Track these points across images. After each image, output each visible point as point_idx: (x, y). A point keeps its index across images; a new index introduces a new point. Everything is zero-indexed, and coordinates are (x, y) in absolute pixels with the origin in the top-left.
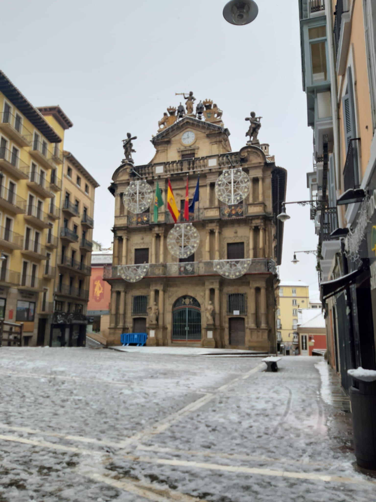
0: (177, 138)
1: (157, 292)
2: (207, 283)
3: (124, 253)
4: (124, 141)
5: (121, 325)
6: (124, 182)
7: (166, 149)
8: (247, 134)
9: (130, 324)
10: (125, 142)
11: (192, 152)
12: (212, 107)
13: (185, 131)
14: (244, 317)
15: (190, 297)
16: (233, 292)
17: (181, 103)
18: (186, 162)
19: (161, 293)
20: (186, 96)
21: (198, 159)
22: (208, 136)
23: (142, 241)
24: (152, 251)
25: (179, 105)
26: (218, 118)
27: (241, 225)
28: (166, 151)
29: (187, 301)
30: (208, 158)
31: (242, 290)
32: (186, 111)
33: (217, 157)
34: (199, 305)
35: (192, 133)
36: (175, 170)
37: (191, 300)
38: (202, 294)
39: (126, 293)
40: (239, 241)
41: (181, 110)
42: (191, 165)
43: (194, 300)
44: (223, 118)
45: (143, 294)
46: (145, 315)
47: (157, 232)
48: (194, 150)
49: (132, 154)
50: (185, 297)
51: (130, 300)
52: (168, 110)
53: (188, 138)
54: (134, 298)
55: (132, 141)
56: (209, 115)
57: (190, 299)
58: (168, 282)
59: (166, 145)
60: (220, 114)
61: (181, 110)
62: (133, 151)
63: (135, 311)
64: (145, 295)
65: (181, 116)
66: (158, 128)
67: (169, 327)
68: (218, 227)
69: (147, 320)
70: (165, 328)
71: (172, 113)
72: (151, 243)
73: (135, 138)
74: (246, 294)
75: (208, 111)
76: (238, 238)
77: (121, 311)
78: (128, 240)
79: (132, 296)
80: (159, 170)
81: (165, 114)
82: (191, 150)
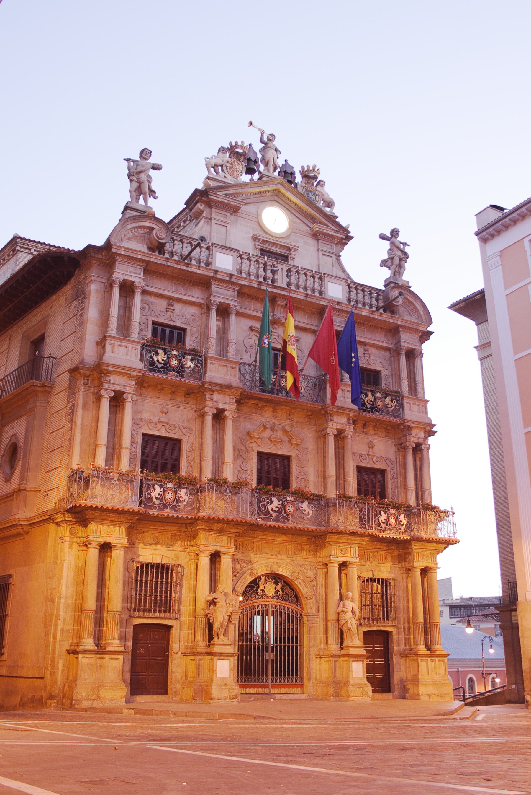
3: (126, 440)
6: (140, 257)
8: (384, 263)
11: (284, 252)
19: (226, 562)
22: (316, 236)
32: (262, 168)
45: (165, 561)
47: (221, 406)
48: (289, 249)
57: (276, 583)
59: (229, 215)
61: (253, 159)
62: (152, 193)
69: (175, 633)
73: (156, 167)
80: (224, 262)
82: (282, 246)
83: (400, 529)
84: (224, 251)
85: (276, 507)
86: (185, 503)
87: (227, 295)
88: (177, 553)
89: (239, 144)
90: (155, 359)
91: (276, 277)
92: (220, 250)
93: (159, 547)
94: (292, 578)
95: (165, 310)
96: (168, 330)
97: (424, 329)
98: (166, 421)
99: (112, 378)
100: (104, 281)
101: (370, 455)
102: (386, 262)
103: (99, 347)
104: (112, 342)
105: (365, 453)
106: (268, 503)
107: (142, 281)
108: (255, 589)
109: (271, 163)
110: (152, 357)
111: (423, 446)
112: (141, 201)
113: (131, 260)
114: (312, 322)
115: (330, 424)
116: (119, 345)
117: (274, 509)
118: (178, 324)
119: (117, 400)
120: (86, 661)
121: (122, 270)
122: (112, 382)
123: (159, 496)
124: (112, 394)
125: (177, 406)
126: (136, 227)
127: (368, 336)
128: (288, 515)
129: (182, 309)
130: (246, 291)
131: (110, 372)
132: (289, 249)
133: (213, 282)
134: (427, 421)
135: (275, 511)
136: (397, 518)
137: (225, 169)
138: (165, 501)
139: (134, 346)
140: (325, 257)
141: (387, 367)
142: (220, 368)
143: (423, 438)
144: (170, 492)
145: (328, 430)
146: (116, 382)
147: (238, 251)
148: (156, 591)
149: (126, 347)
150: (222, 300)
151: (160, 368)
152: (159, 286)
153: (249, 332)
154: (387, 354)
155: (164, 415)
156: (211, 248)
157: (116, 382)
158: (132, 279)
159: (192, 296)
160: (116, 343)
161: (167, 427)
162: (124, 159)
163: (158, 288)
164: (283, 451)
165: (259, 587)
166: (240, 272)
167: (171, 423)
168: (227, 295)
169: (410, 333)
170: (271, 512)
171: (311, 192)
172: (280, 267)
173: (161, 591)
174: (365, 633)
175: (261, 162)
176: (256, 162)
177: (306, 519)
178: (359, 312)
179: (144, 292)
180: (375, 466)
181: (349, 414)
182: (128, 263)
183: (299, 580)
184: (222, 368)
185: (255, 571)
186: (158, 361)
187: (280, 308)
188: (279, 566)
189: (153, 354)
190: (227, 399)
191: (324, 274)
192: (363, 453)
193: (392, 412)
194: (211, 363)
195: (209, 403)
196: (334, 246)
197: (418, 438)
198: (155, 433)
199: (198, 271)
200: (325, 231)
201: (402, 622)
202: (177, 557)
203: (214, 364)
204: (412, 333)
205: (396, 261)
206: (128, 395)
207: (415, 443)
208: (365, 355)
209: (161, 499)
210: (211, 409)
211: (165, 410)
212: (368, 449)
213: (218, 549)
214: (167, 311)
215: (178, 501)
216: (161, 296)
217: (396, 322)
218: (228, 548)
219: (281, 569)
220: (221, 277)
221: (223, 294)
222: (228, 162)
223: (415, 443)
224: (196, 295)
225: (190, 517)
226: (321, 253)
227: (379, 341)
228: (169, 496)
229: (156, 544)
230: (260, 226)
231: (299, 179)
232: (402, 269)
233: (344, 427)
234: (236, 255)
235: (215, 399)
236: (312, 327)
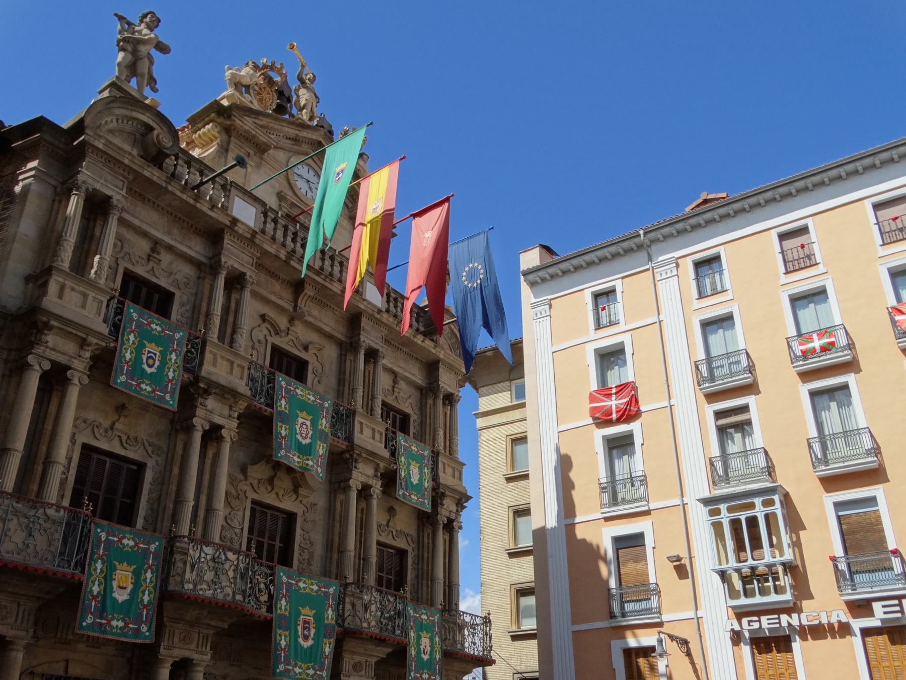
4: (121, 18)
6: (126, 161)
73: (162, 48)
80: (245, 213)
84: (246, 198)
95: (145, 257)
96: (144, 290)
100: (54, 183)
103: (31, 285)
104: (61, 280)
105: (384, 523)
107: (123, 200)
111: (455, 524)
113: (111, 161)
115: (355, 474)
116: (73, 289)
118: (163, 282)
122: (50, 344)
124: (47, 366)
126: (126, 116)
127: (402, 365)
129: (171, 263)
130: (267, 262)
134: (462, 490)
137: (251, 91)
139: (98, 297)
145: (351, 482)
146: (55, 347)
147: (264, 204)
153: (259, 321)
156: (229, 187)
158: (108, 192)
160: (69, 284)
162: (116, 15)
164: (288, 504)
179: (122, 221)
195: (200, 412)
197: (450, 512)
199: (209, 212)
206: (75, 373)
210: (203, 422)
216: (145, 234)
220: (240, 231)
224: (196, 248)
233: (370, 483)
234: (261, 209)
235: (209, 407)
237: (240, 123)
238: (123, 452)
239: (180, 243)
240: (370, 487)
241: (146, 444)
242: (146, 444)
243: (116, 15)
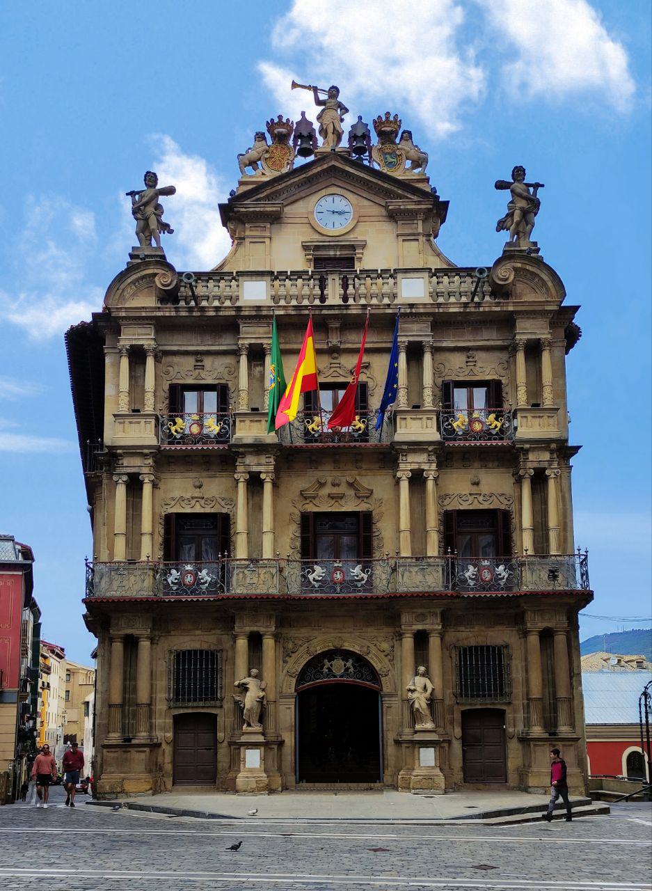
0: (299, 208)
1: (255, 641)
2: (405, 618)
3: (146, 525)
4: (132, 194)
5: (142, 736)
7: (268, 234)
8: (501, 226)
9: (164, 732)
10: (137, 197)
11: (345, 253)
12: (397, 141)
13: (323, 192)
14: (504, 707)
15: (346, 655)
16: (473, 643)
17: (303, 114)
18: (336, 277)
19: (268, 643)
20: (323, 97)
21: (368, 273)
22: (393, 216)
23: (197, 493)
24: (241, 523)
25: (299, 118)
26: (417, 171)
27: (490, 465)
28: (267, 241)
29: (338, 666)
30: (399, 276)
31: (499, 636)
32: (320, 140)
33: (426, 275)
34: (375, 676)
35: (344, 202)
36: (303, 293)
37: (349, 664)
38: (385, 646)
39: (152, 640)
40: (485, 506)
41: (305, 133)
42: (351, 290)
43: (361, 662)
44: (429, 171)
45: (205, 647)
46: (215, 707)
47: (255, 469)
48: (353, 247)
49: (164, 237)
50: (331, 655)
51: (164, 666)
52: (271, 126)
53: (333, 213)
54: (178, 655)
55: (162, 200)
56: (390, 160)
58: (286, 612)
60: (420, 162)
61: (305, 133)
62: (166, 227)
63: (179, 694)
64: (212, 648)
65: (304, 152)
66: (239, 176)
67: (289, 739)
68: (434, 466)
69: (220, 720)
70: (281, 744)
71: (281, 139)
72: (233, 502)
73: (170, 191)
74: (507, 646)
75: (388, 148)
76: (481, 498)
77: (143, 696)
78: (155, 486)
79: (170, 652)
80: (255, 293)
81: (260, 137)
82: (343, 247)
83: (499, 584)
85: (319, 577)
86: (207, 585)
87: (259, 333)
88: (220, 636)
89: (276, 120)
90: (173, 429)
91: (325, 292)
92: (249, 278)
93: (198, 632)
94: (362, 654)
95: (192, 368)
97: (555, 308)
98: (201, 495)
99: (126, 461)
101: (473, 494)
102: (504, 222)
106: (309, 572)
108: (319, 668)
109: (330, 130)
110: (169, 429)
112: (154, 244)
113: (139, 320)
114: (385, 338)
115: (402, 466)
116: (130, 423)
117: (317, 578)
119: (134, 485)
120: (112, 755)
121: (129, 335)
123: (176, 581)
124: (125, 478)
125: (214, 477)
128: (335, 583)
129: (213, 362)
130: (287, 320)
131: (120, 455)
132: (354, 248)
133: (240, 321)
135: (317, 581)
136: (492, 571)
138: (184, 585)
139: (147, 420)
140: (406, 243)
141: (503, 372)
142: (252, 424)
143: (548, 461)
144: (189, 575)
148: (184, 679)
149: (139, 423)
150: (253, 341)
151: (180, 439)
152: (177, 343)
154: (497, 355)
155: (198, 490)
157: (130, 464)
158: (140, 343)
159: (219, 345)
160: (127, 421)
161: (202, 502)
163: (180, 345)
165: (324, 665)
166: (275, 298)
167: (205, 497)
168: (259, 333)
169: (533, 318)
170: (313, 582)
171: (389, 153)
172: (330, 277)
173: (190, 679)
174: (463, 713)
175: (320, 132)
176: (311, 137)
177: (359, 585)
178: (446, 310)
180: (481, 507)
181: (427, 449)
182: (135, 324)
183: (370, 655)
184: (255, 424)
185: (312, 649)
186: (176, 431)
187: (335, 331)
188: (345, 641)
189: (170, 425)
190: (263, 459)
191: (395, 270)
192: (463, 493)
193: (497, 434)
194: (240, 421)
195: (240, 469)
196: (420, 223)
198: (188, 510)
200: (402, 207)
201: (521, 699)
202: (220, 641)
203: (244, 421)
204: (535, 318)
205: (517, 218)
206: (145, 476)
207: (533, 469)
208: (469, 364)
209: (180, 583)
211: (197, 484)
212: (470, 486)
213: (255, 629)
214: (195, 369)
215: (199, 584)
217: (505, 309)
218: (267, 627)
219: (346, 644)
220: (247, 313)
221: (254, 333)
222: (267, 152)
223: (533, 469)
224: (225, 343)
225: (212, 599)
226: (401, 239)
227: (488, 340)
228: (189, 579)
229: (194, 629)
230: (313, 228)
231: (375, 140)
232: (529, 226)
234: (269, 278)
236: (384, 345)
237: (243, 210)
238: (202, 511)
239: (212, 345)
240: (423, 470)
241: (220, 500)
242: (220, 500)
243: (127, 194)
